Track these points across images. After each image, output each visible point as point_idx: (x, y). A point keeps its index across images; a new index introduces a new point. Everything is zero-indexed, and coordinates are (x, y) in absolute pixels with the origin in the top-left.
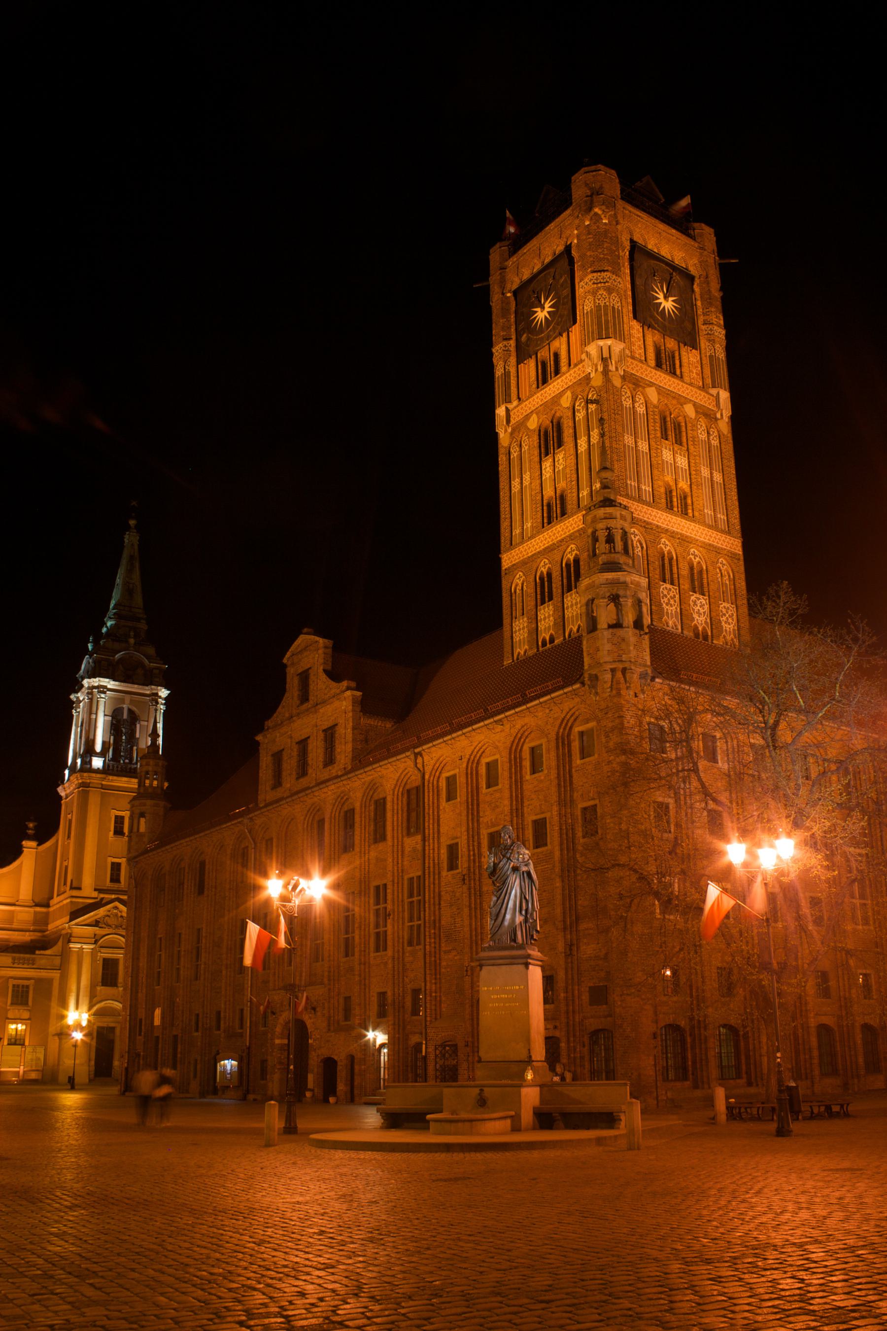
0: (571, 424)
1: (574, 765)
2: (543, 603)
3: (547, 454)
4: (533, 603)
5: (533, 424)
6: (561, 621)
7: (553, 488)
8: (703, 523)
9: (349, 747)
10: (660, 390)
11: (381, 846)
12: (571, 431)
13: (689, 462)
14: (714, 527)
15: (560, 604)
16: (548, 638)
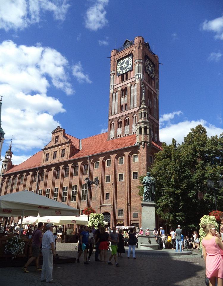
0: (130, 90)
1: (132, 163)
2: (119, 128)
3: (122, 96)
4: (116, 128)
5: (120, 89)
6: (123, 132)
7: (123, 103)
8: (153, 117)
9: (69, 154)
10: (148, 87)
11: (75, 177)
12: (130, 92)
13: (152, 104)
14: (155, 118)
15: (123, 129)
16: (119, 136)
